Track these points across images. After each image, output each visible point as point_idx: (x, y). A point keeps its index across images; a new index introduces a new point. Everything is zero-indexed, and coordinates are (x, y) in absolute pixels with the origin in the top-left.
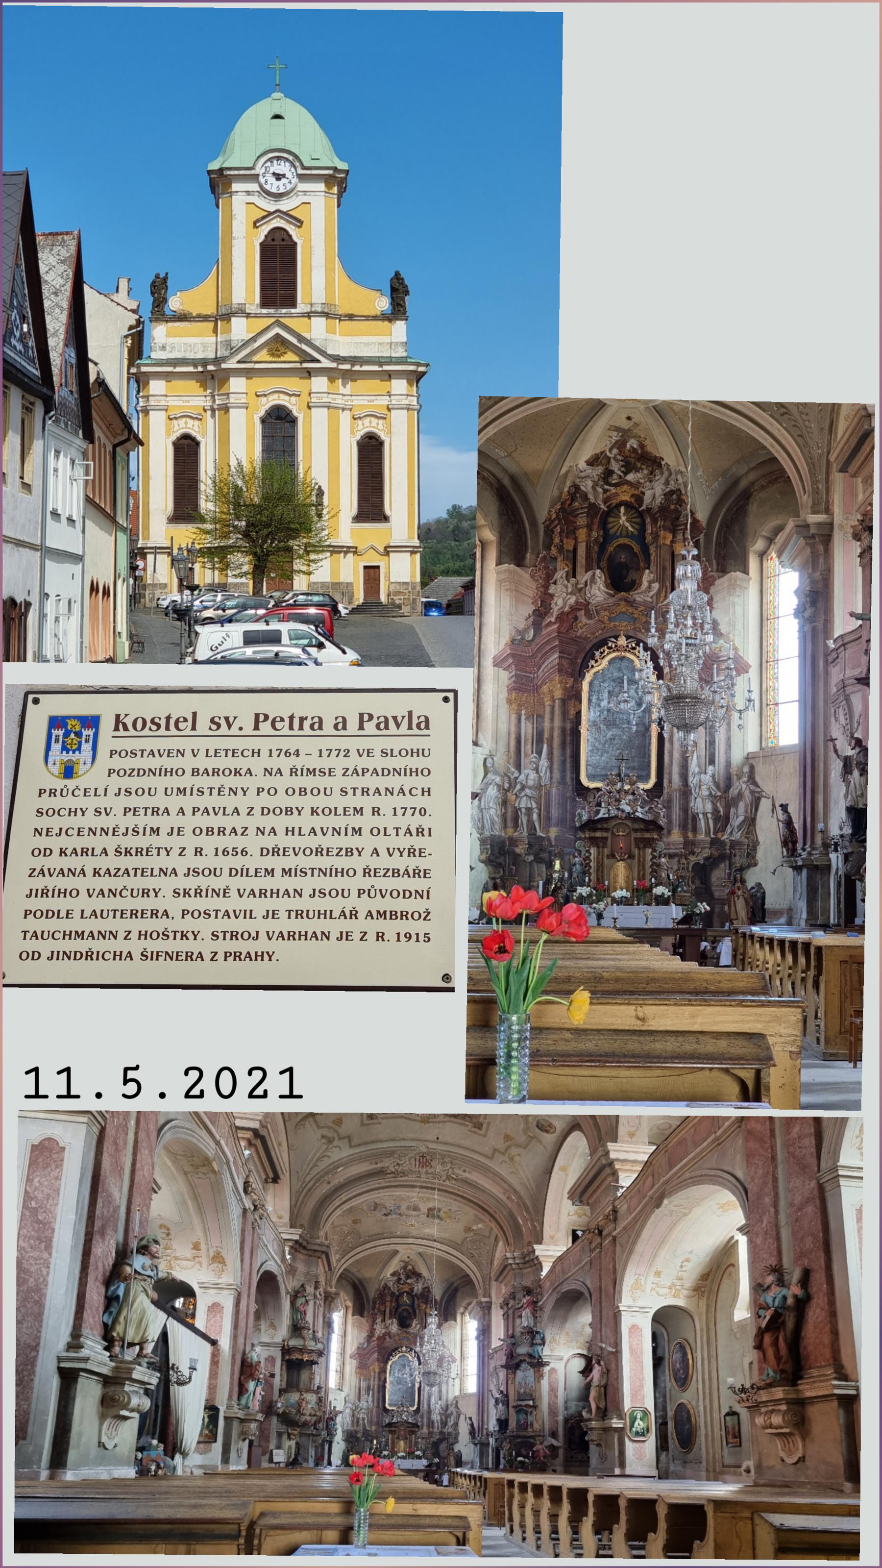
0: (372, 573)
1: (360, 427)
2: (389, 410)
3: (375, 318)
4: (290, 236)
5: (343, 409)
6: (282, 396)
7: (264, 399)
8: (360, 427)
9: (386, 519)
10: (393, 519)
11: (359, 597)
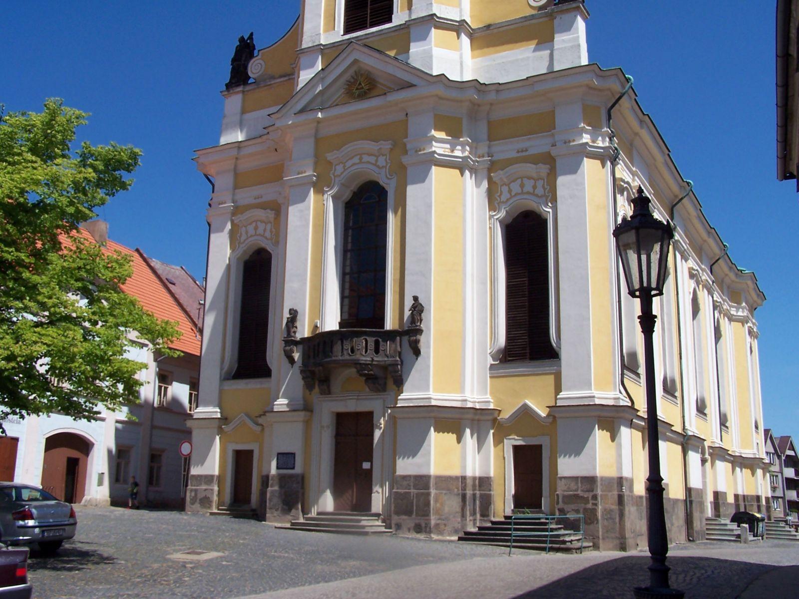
11: (503, 504)
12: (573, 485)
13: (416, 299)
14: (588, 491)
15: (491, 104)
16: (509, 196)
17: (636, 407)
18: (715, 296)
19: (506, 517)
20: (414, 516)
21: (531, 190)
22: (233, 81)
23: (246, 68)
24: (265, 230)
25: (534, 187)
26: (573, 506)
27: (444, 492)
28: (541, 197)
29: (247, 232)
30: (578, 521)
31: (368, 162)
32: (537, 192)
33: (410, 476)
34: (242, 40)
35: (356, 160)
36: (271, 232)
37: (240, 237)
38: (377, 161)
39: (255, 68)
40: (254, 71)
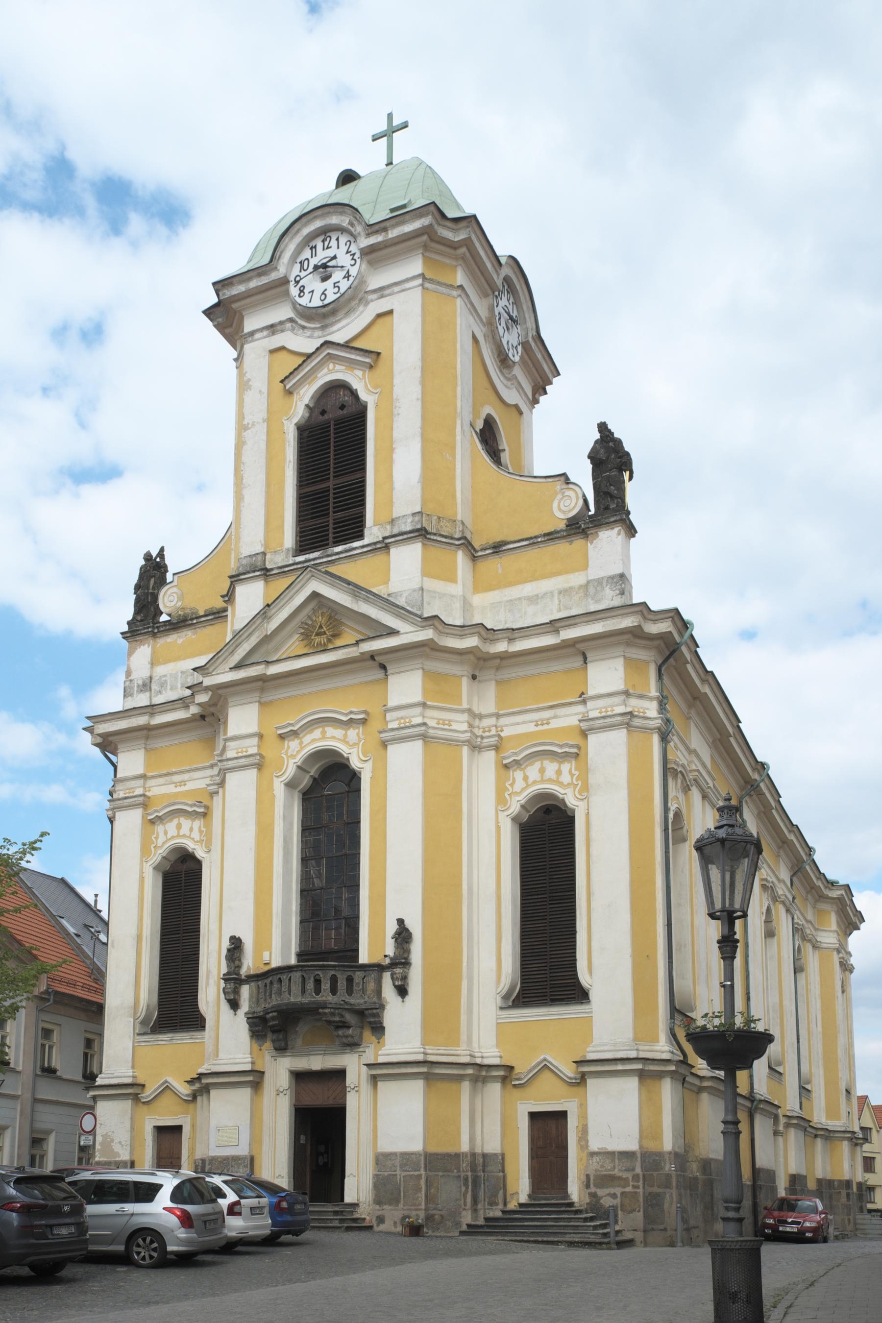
0: (548, 1128)
1: (519, 784)
2: (584, 734)
3: (551, 537)
4: (354, 394)
5: (476, 748)
6: (331, 731)
7: (293, 745)
8: (519, 784)
9: (580, 995)
10: (592, 996)
13: (401, 922)
14: (627, 1170)
16: (524, 785)
17: (689, 1062)
18: (795, 917)
19: (521, 1205)
20: (401, 1206)
21: (554, 777)
22: (139, 618)
23: (155, 598)
24: (191, 830)
25: (559, 772)
26: (607, 1191)
27: (441, 1174)
28: (569, 784)
29: (166, 833)
30: (615, 1208)
31: (333, 738)
32: (562, 779)
33: (395, 1154)
34: (148, 557)
35: (317, 733)
36: (201, 832)
37: (157, 838)
38: (345, 735)
39: (169, 601)
40: (166, 600)
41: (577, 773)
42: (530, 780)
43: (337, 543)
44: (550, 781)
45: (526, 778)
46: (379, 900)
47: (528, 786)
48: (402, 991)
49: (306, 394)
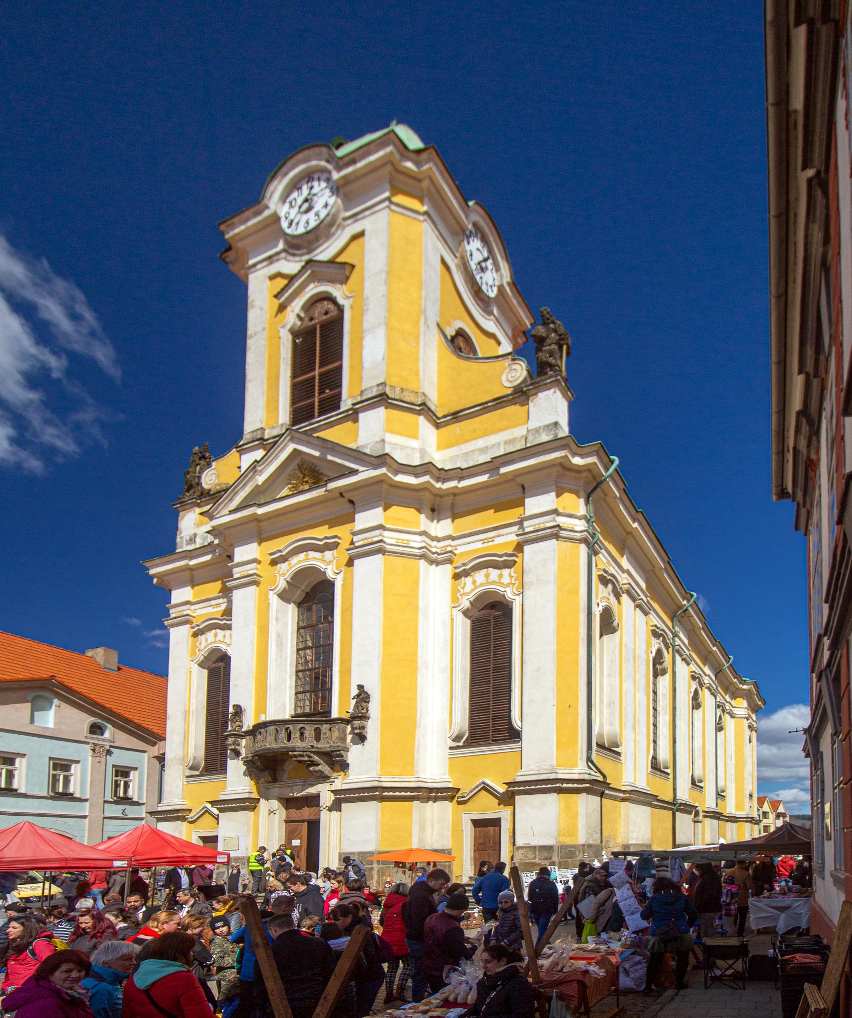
3: (499, 402)
9: (515, 735)
10: (524, 736)
12: (530, 855)
14: (546, 859)
15: (455, 495)
16: (473, 587)
25: (501, 576)
28: (508, 585)
38: (323, 556)
41: (515, 575)
42: (478, 583)
43: (319, 416)
44: (494, 582)
45: (474, 582)
46: (346, 672)
47: (476, 588)
48: (361, 738)
49: (297, 306)
